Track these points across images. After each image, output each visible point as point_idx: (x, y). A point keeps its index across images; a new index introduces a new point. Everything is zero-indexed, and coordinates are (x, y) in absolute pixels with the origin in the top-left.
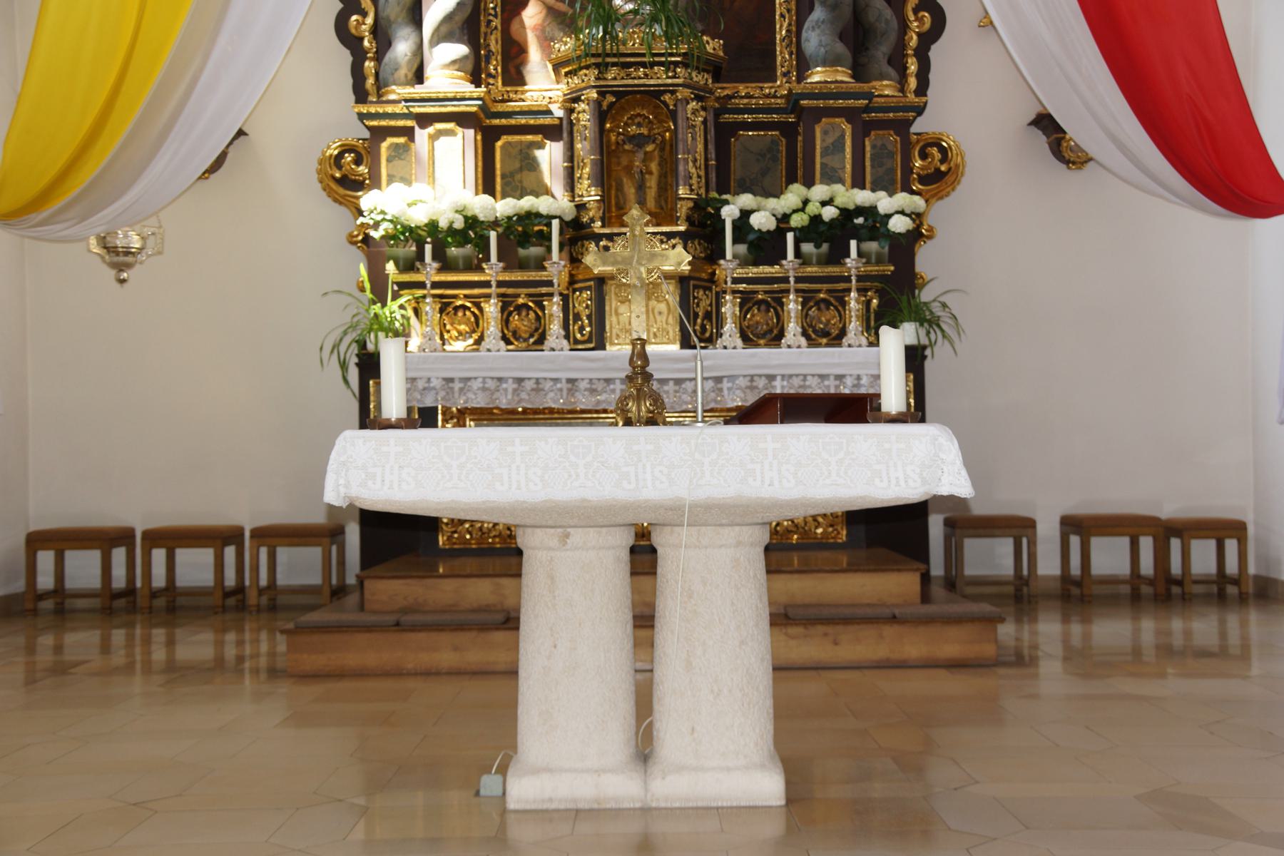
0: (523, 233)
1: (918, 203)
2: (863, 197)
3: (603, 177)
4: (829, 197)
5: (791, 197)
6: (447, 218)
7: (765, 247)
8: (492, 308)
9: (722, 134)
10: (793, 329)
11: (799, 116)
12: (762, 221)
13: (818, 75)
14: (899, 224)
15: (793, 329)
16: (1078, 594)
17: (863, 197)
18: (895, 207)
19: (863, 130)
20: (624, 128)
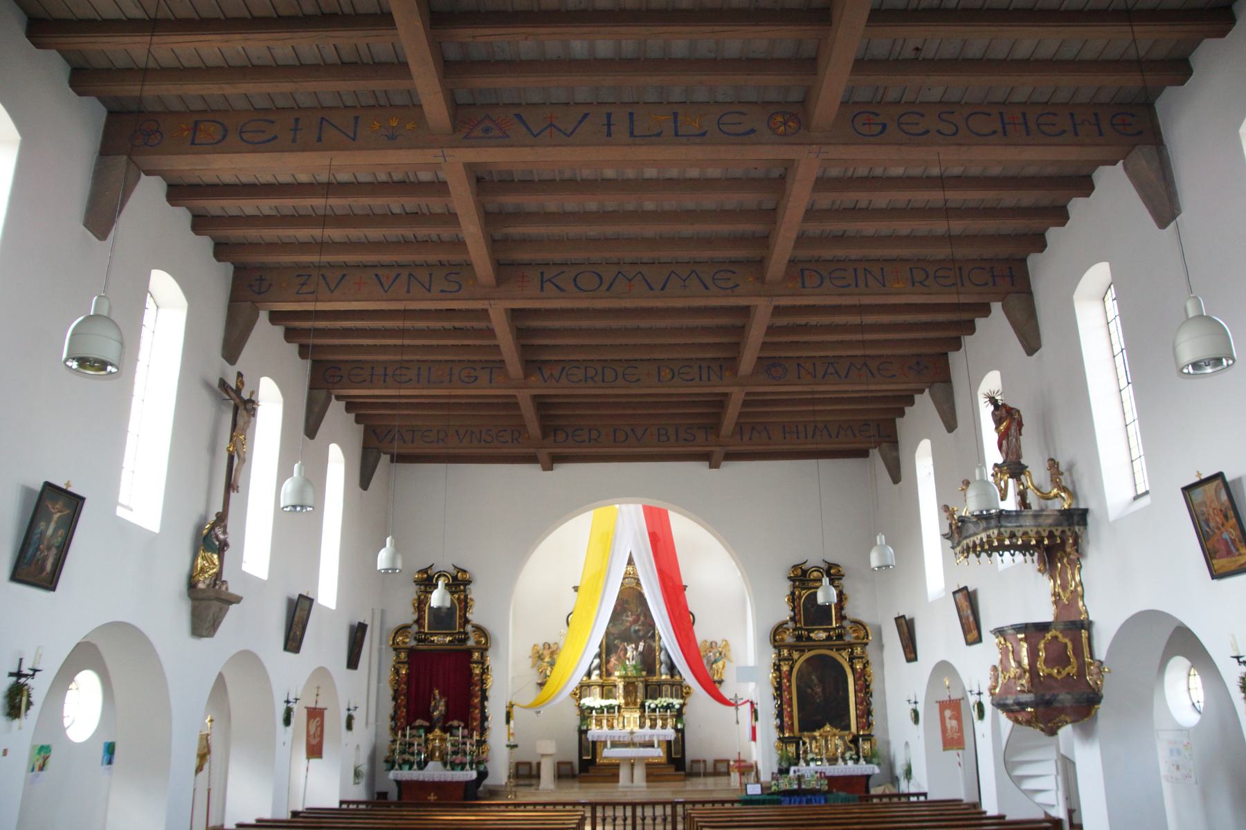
0: (610, 708)
1: (681, 701)
2: (671, 700)
3: (625, 697)
4: (663, 701)
5: (657, 702)
6: (597, 706)
7: (654, 710)
8: (605, 722)
9: (646, 686)
10: (659, 723)
11: (660, 684)
12: (653, 706)
13: (664, 677)
14: (677, 706)
15: (659, 723)
16: (716, 773)
17: (671, 700)
18: (677, 702)
19: (672, 685)
20: (630, 688)
